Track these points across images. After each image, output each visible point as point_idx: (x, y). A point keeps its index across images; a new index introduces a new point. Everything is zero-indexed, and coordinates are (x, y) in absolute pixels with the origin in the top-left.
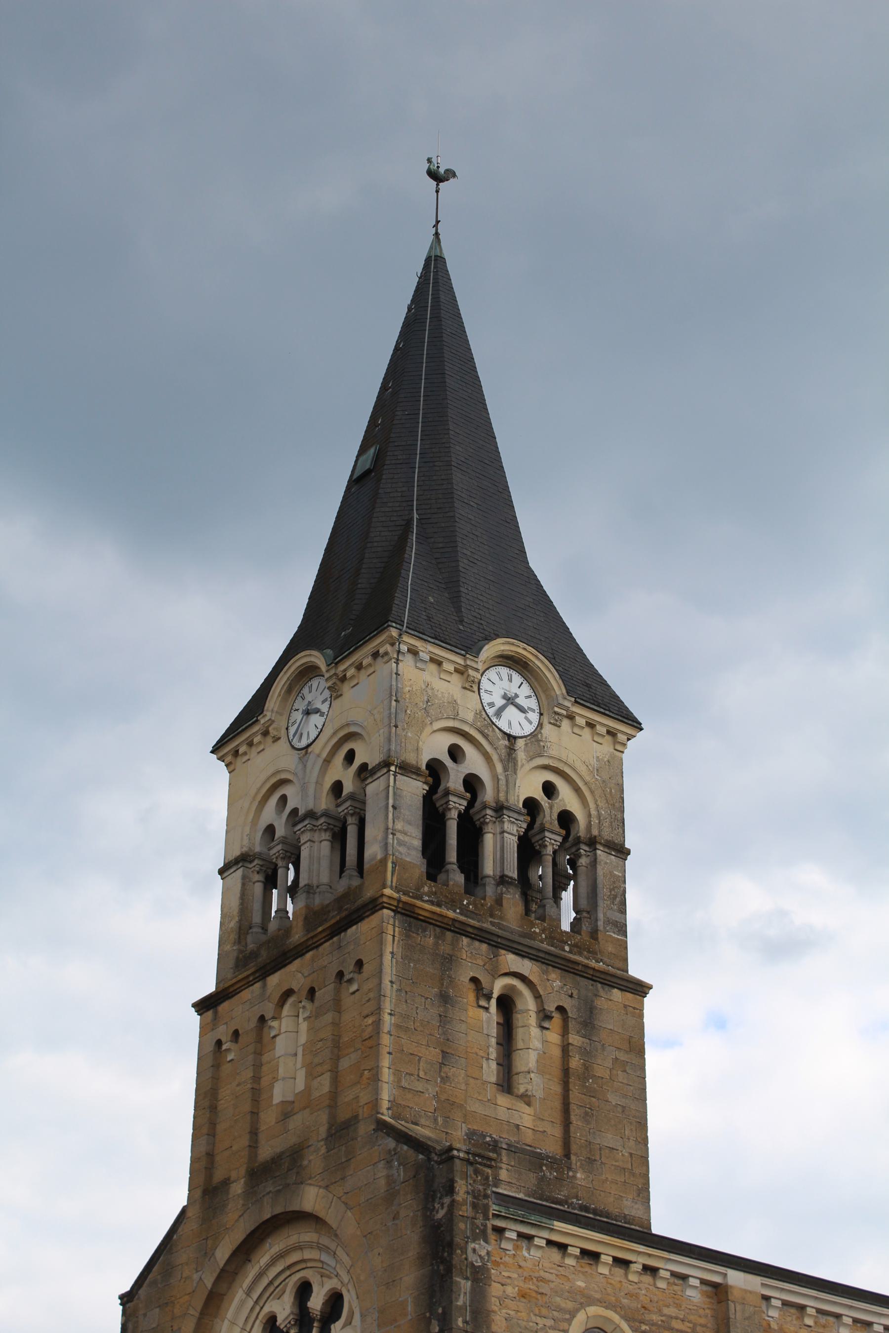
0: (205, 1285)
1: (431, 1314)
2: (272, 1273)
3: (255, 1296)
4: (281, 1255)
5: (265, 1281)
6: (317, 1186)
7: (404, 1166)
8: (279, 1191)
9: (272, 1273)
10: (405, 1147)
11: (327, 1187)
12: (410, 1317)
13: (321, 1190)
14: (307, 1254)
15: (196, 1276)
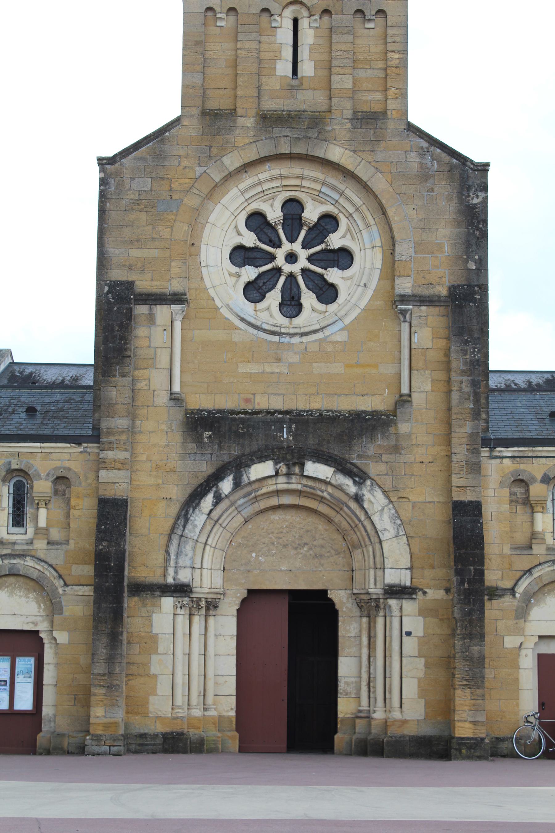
0: (212, 179)
1: (468, 257)
2: (266, 186)
3: (247, 196)
4: (281, 177)
5: (259, 189)
6: (343, 148)
7: (438, 161)
8: (299, 139)
9: (266, 186)
10: (439, 150)
11: (354, 151)
12: (446, 254)
13: (347, 152)
14: (305, 183)
15: (199, 170)
